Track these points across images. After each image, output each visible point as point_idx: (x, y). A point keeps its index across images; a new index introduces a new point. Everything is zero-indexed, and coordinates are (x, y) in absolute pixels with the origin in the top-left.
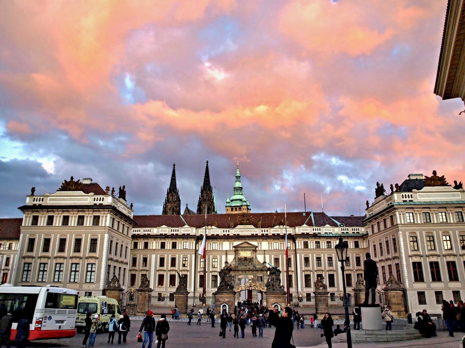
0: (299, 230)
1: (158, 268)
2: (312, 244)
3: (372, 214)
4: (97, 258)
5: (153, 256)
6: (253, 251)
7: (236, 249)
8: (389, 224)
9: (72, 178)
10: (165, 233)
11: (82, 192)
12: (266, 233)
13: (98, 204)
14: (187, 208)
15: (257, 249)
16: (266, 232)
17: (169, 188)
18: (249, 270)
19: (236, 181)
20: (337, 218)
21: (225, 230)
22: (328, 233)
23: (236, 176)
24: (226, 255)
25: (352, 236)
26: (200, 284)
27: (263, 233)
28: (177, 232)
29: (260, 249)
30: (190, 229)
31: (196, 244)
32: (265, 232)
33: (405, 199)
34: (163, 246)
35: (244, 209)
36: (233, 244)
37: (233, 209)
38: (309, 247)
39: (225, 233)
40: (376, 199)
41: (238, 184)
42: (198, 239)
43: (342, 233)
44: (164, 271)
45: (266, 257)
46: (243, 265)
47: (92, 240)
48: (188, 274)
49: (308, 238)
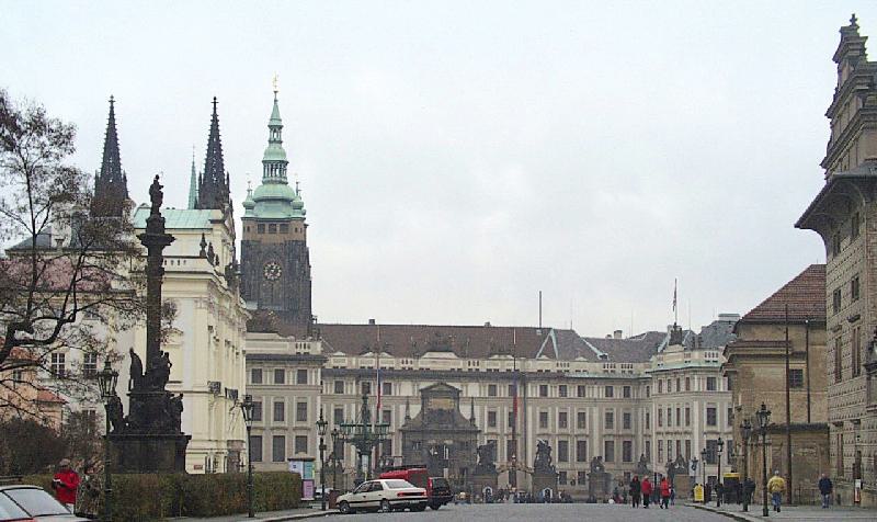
0: (533, 366)
2: (553, 392)
7: (425, 395)
8: (683, 388)
18: (446, 432)
20: (595, 342)
24: (408, 404)
27: (471, 367)
33: (707, 359)
38: (549, 395)
42: (362, 375)
49: (549, 379)
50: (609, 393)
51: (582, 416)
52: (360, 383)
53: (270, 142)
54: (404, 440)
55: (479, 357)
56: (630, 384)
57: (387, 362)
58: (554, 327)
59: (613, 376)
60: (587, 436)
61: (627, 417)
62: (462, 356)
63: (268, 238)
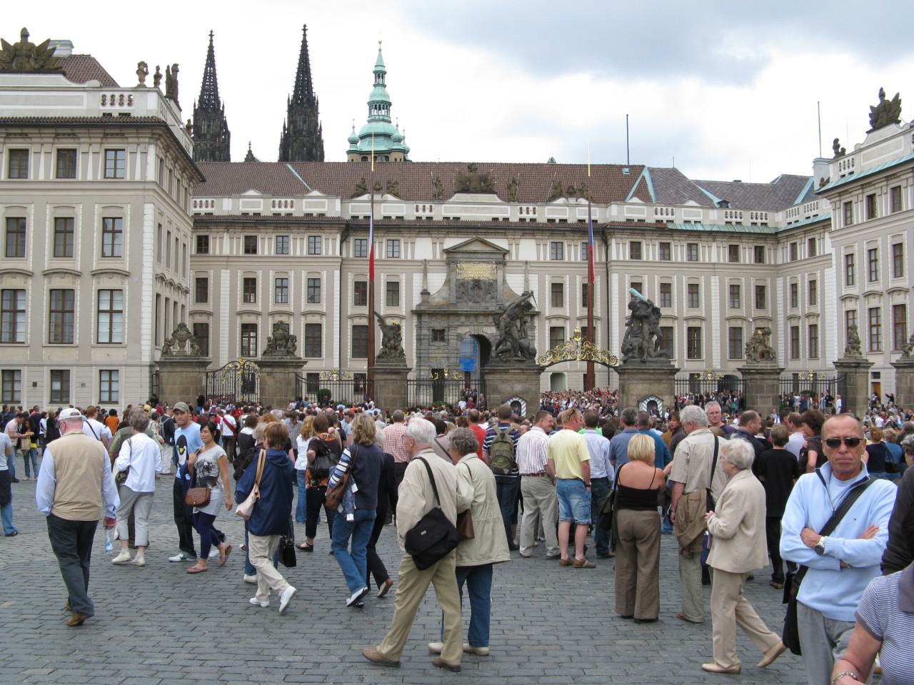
1: (240, 306)
3: (852, 173)
4: (125, 275)
5: (225, 275)
6: (496, 263)
9: (25, 34)
10: (257, 210)
11: (61, 76)
12: (531, 215)
13: (115, 115)
14: (250, 152)
15: (507, 258)
16: (531, 213)
18: (486, 315)
20: (710, 185)
21: (421, 206)
22: (693, 223)
25: (750, 233)
26: (354, 347)
27: (524, 215)
28: (289, 210)
29: (514, 258)
30: (326, 200)
31: (341, 242)
32: (528, 213)
34: (251, 248)
36: (442, 243)
38: (644, 258)
39: (420, 213)
40: (871, 135)
42: (350, 228)
43: (727, 222)
44: (258, 314)
45: (530, 278)
46: (470, 300)
48: (324, 322)
50: (734, 251)
51: (694, 289)
52: (352, 240)
53: (375, 86)
54: (419, 327)
55: (534, 201)
56: (764, 240)
57: (391, 207)
58: (647, 165)
59: (738, 229)
60: (702, 319)
61: (760, 291)
62: (510, 197)
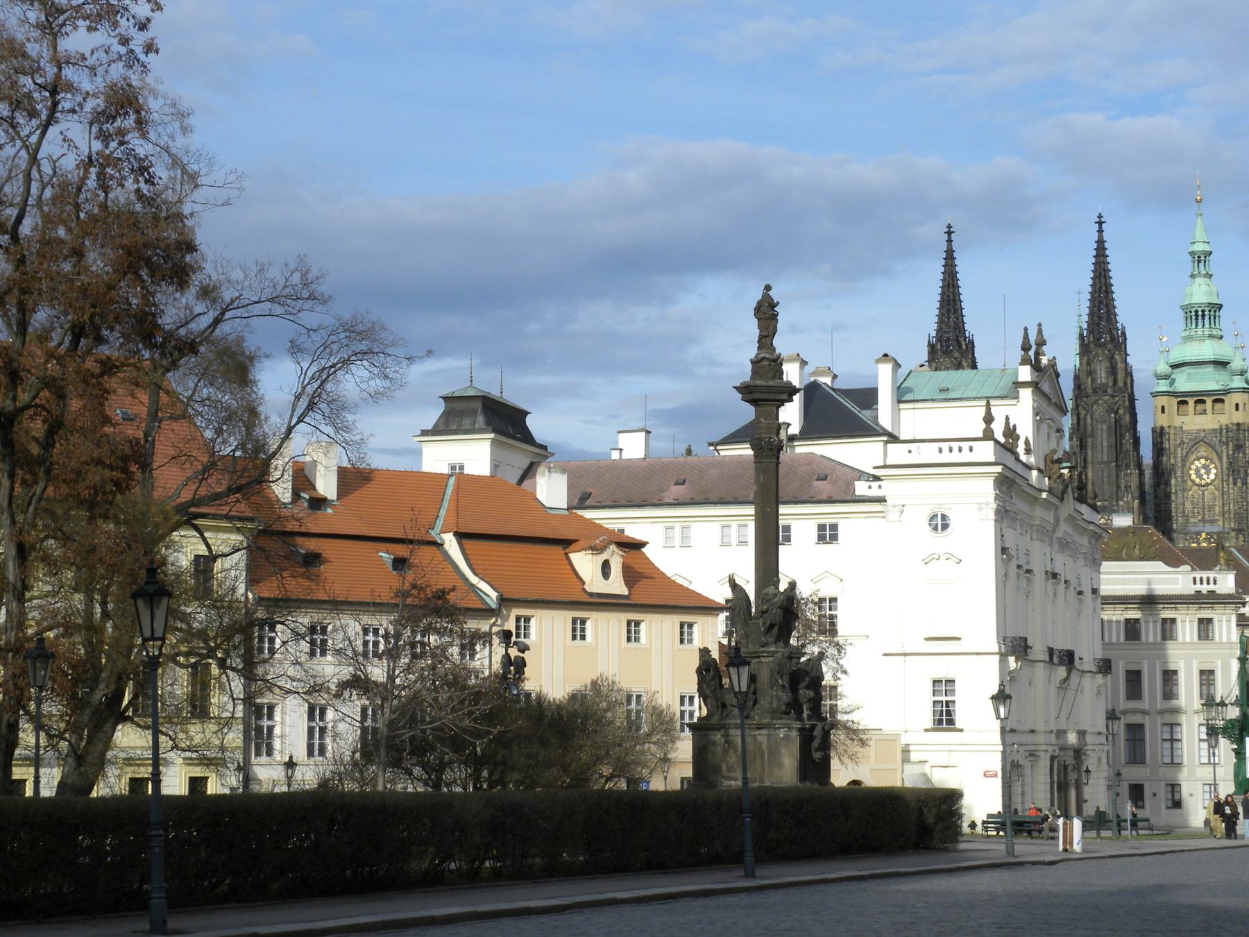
11: (1161, 563)
17: (934, 334)
19: (1193, 276)
23: (1192, 254)
35: (1237, 405)
37: (1186, 402)
41: (1204, 288)
47: (1202, 672)
63: (1195, 422)
